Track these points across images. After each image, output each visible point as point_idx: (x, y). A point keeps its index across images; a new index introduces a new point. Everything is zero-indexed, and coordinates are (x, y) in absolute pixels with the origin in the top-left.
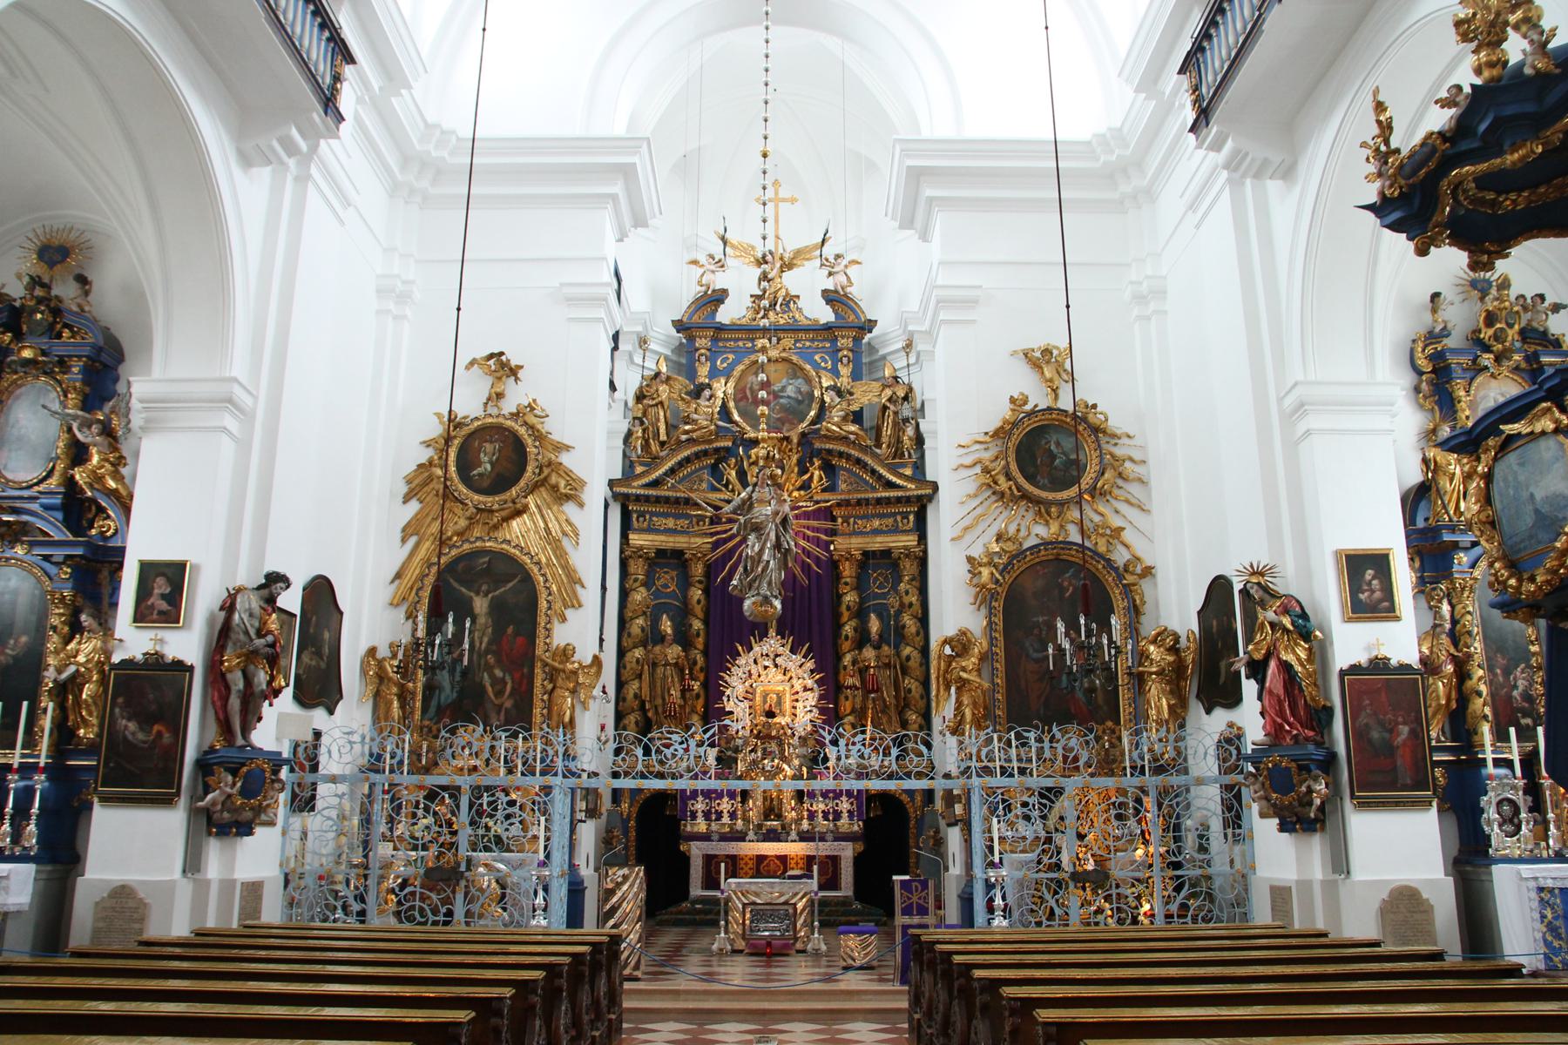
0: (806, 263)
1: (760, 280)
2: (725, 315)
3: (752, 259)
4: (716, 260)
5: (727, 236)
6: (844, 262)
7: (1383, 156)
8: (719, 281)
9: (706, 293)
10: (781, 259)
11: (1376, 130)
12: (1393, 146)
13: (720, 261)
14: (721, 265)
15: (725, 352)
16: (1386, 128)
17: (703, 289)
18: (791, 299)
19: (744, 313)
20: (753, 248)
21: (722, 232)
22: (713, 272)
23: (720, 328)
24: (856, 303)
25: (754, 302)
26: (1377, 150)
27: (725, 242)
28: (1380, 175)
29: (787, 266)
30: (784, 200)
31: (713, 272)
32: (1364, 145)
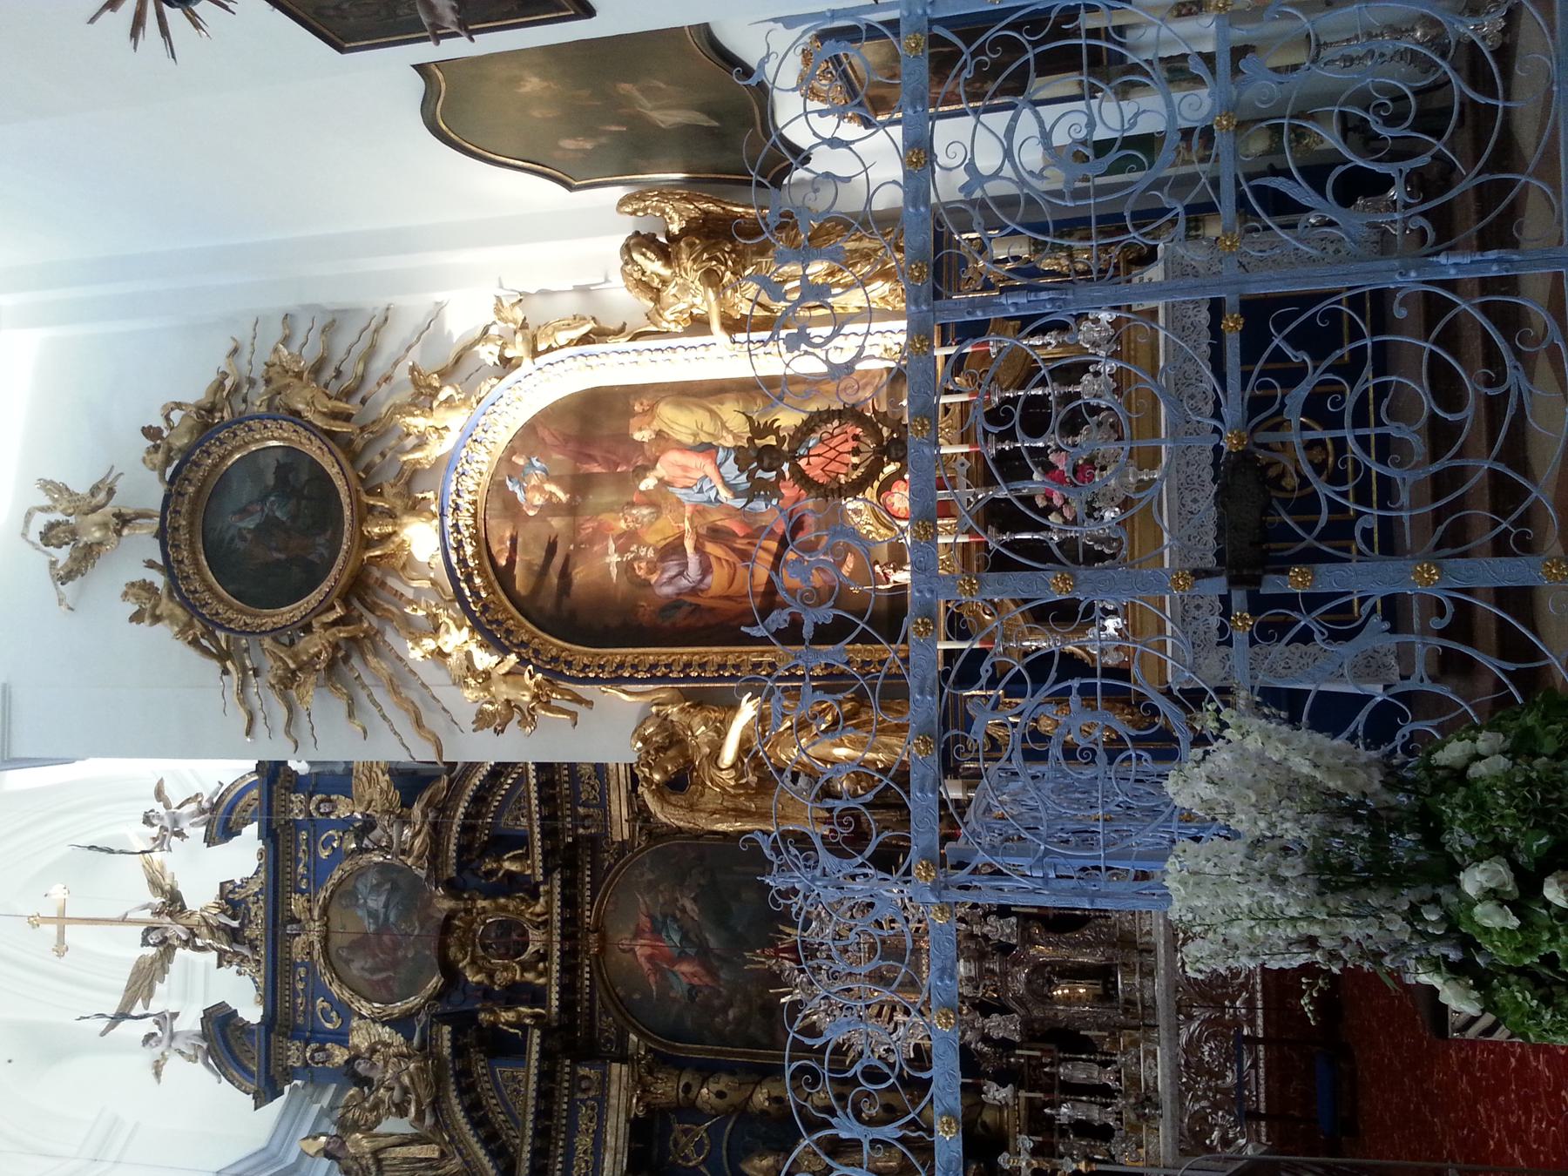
0: (168, 871)
2: (252, 1013)
4: (155, 1029)
8: (190, 1021)
10: (158, 913)
13: (157, 1023)
15: (314, 1013)
18: (230, 898)
19: (247, 980)
23: (269, 1021)
25: (230, 963)
27: (122, 1015)
29: (173, 902)
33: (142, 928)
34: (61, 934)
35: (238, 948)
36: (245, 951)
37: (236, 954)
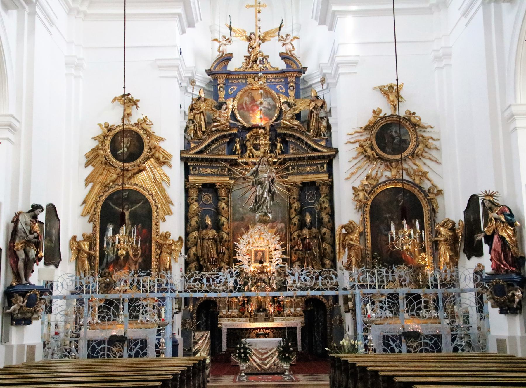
0: (272, 39)
1: (248, 48)
2: (232, 66)
3: (245, 38)
4: (227, 38)
5: (232, 26)
6: (291, 38)
8: (228, 49)
9: (222, 55)
13: (228, 39)
14: (229, 40)
15: (232, 85)
17: (221, 53)
19: (241, 65)
20: (245, 32)
21: (229, 24)
22: (225, 45)
23: (230, 73)
24: (297, 59)
25: (246, 60)
27: (230, 28)
29: (264, 41)
31: (225, 45)
33: (255, 33)
34: (252, 6)
35: (251, 63)
36: (250, 65)
37: (249, 62)
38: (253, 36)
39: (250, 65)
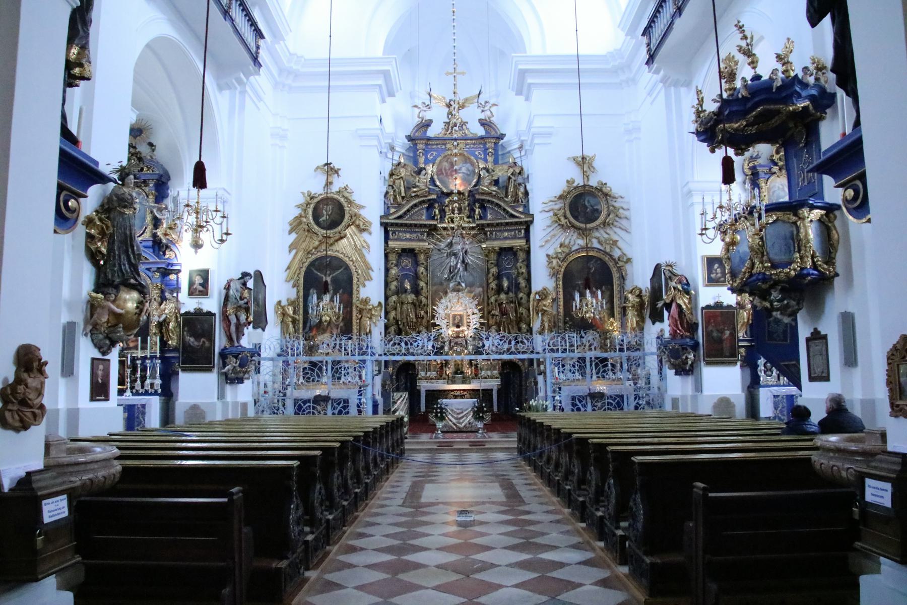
0: (471, 105)
2: (432, 132)
5: (432, 93)
7: (698, 113)
8: (428, 115)
11: (697, 102)
12: (704, 108)
16: (701, 102)
18: (463, 124)
19: (440, 131)
23: (429, 139)
26: (698, 110)
28: (696, 122)
29: (462, 107)
30: (459, 73)
32: (693, 107)
36: (450, 131)
38: (452, 103)
39: (450, 131)
